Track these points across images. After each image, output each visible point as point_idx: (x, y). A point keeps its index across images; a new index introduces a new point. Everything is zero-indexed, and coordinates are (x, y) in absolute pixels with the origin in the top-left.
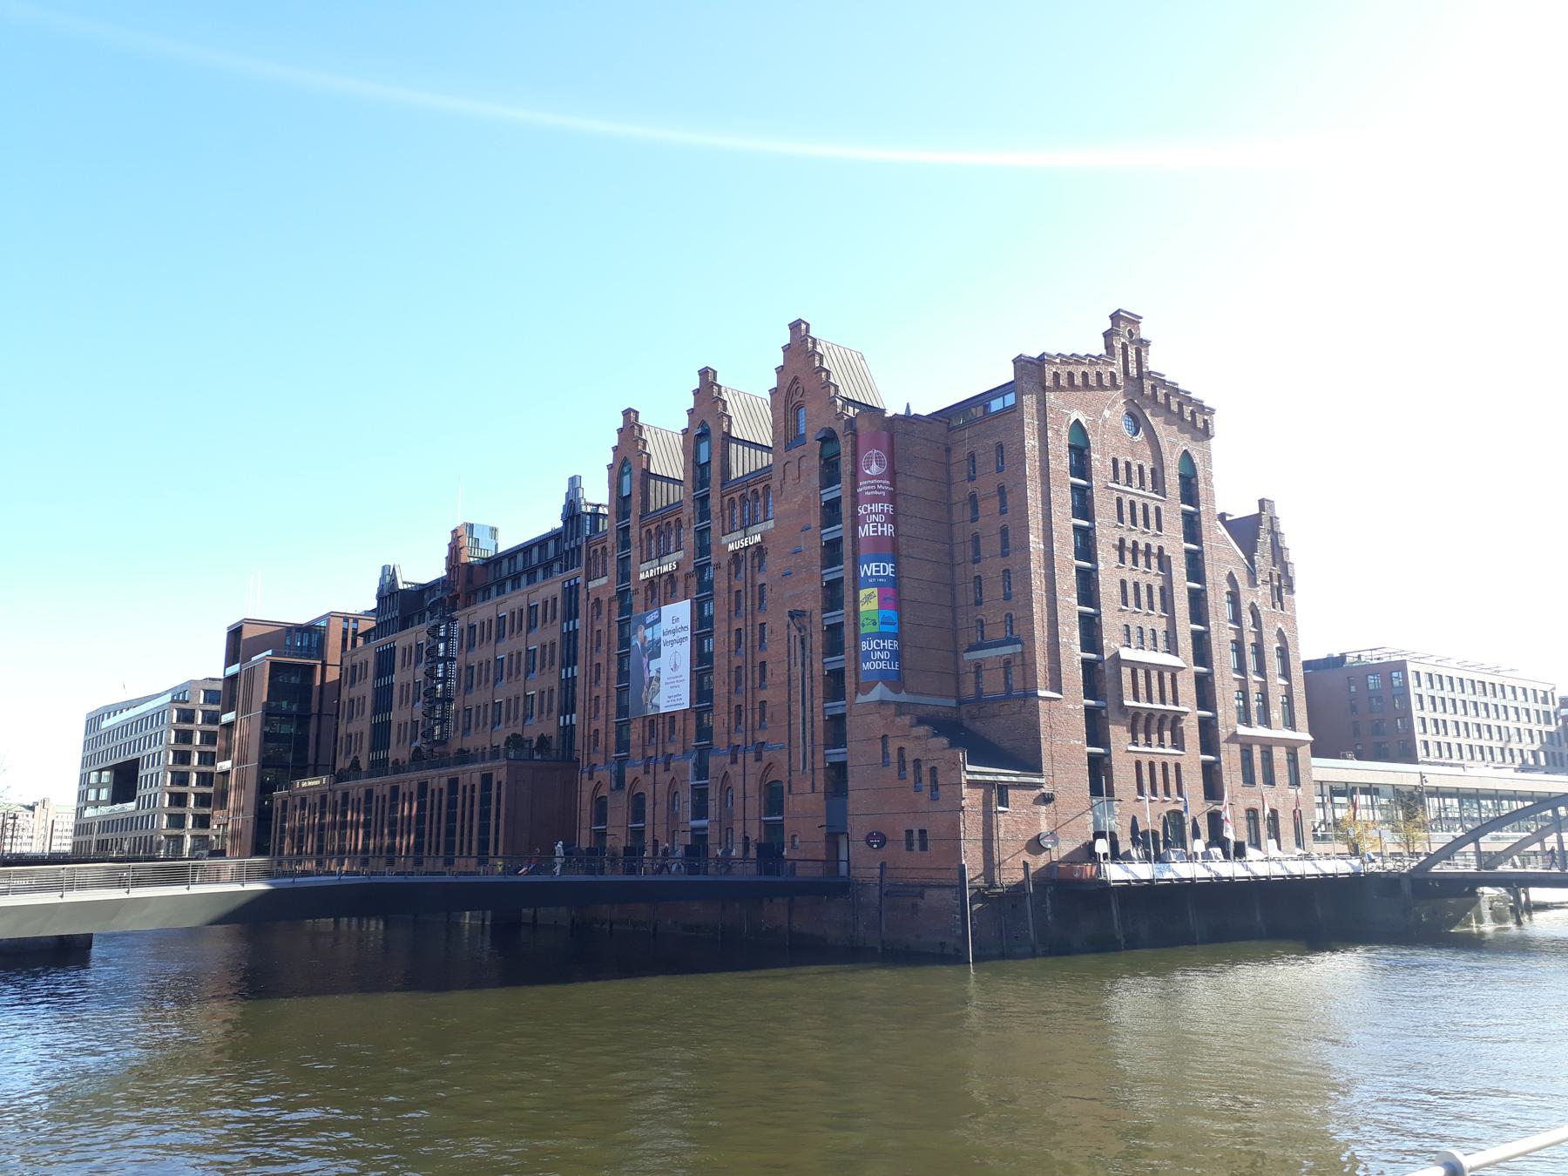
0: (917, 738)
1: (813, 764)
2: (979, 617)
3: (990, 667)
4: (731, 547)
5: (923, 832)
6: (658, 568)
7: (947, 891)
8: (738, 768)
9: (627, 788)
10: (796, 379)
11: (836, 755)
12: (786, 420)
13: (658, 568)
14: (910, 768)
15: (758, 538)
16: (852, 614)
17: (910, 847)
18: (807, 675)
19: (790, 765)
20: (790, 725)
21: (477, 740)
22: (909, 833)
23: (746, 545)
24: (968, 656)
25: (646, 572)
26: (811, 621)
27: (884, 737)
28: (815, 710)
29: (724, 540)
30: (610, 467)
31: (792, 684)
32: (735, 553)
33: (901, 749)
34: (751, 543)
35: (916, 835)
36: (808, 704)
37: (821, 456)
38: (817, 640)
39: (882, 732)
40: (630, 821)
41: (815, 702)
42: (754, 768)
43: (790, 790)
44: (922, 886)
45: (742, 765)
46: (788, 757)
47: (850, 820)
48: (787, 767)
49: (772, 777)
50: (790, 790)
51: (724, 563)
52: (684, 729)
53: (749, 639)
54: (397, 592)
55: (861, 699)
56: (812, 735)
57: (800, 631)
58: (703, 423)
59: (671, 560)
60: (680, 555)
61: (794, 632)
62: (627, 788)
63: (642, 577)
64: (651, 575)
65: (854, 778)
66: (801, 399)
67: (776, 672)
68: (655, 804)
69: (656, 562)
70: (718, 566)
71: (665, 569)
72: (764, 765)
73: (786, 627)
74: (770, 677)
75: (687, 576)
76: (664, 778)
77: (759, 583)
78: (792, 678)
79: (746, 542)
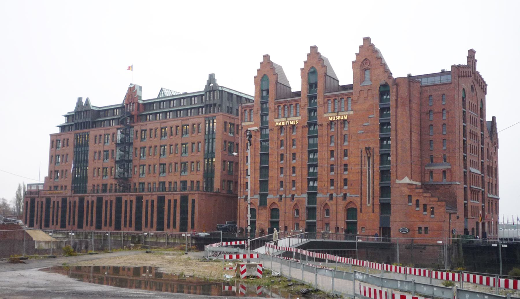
0: (426, 197)
1: (373, 203)
2: (431, 155)
3: (437, 172)
4: (330, 119)
5: (426, 228)
6: (287, 122)
7: (436, 247)
8: (333, 202)
9: (268, 206)
10: (366, 59)
11: (385, 199)
12: (360, 74)
13: (287, 122)
14: (421, 207)
15: (346, 117)
16: (395, 151)
17: (420, 233)
18: (371, 171)
19: (361, 203)
20: (361, 188)
21: (148, 179)
22: (420, 228)
23: (339, 119)
24: (426, 168)
25: (279, 122)
26: (373, 152)
27: (410, 196)
28: (374, 184)
29: (325, 115)
30: (255, 77)
31: (363, 174)
32: (331, 122)
33: (417, 201)
34: (341, 119)
35: (423, 229)
36: (371, 182)
37: (379, 91)
38: (377, 158)
39: (409, 194)
40: (270, 218)
41: (375, 181)
42: (342, 204)
43: (361, 211)
44: (424, 245)
45: (335, 202)
46: (360, 199)
47: (391, 223)
48: (360, 203)
49: (351, 206)
50: (361, 211)
51: (325, 124)
52: (302, 186)
53: (339, 155)
54: (89, 110)
55: (398, 181)
56: (373, 192)
57: (367, 154)
58: (312, 67)
59: (294, 119)
60: (299, 118)
61: (364, 154)
62: (268, 206)
63: (277, 124)
64: (283, 124)
65: (393, 209)
66: (368, 67)
67: (354, 168)
68: (285, 213)
69: (284, 119)
70: (322, 125)
71: (291, 123)
72: (347, 202)
73: (360, 152)
74: (350, 170)
75: (303, 127)
76: (290, 204)
77: (344, 134)
78: (363, 171)
79: (339, 118)
